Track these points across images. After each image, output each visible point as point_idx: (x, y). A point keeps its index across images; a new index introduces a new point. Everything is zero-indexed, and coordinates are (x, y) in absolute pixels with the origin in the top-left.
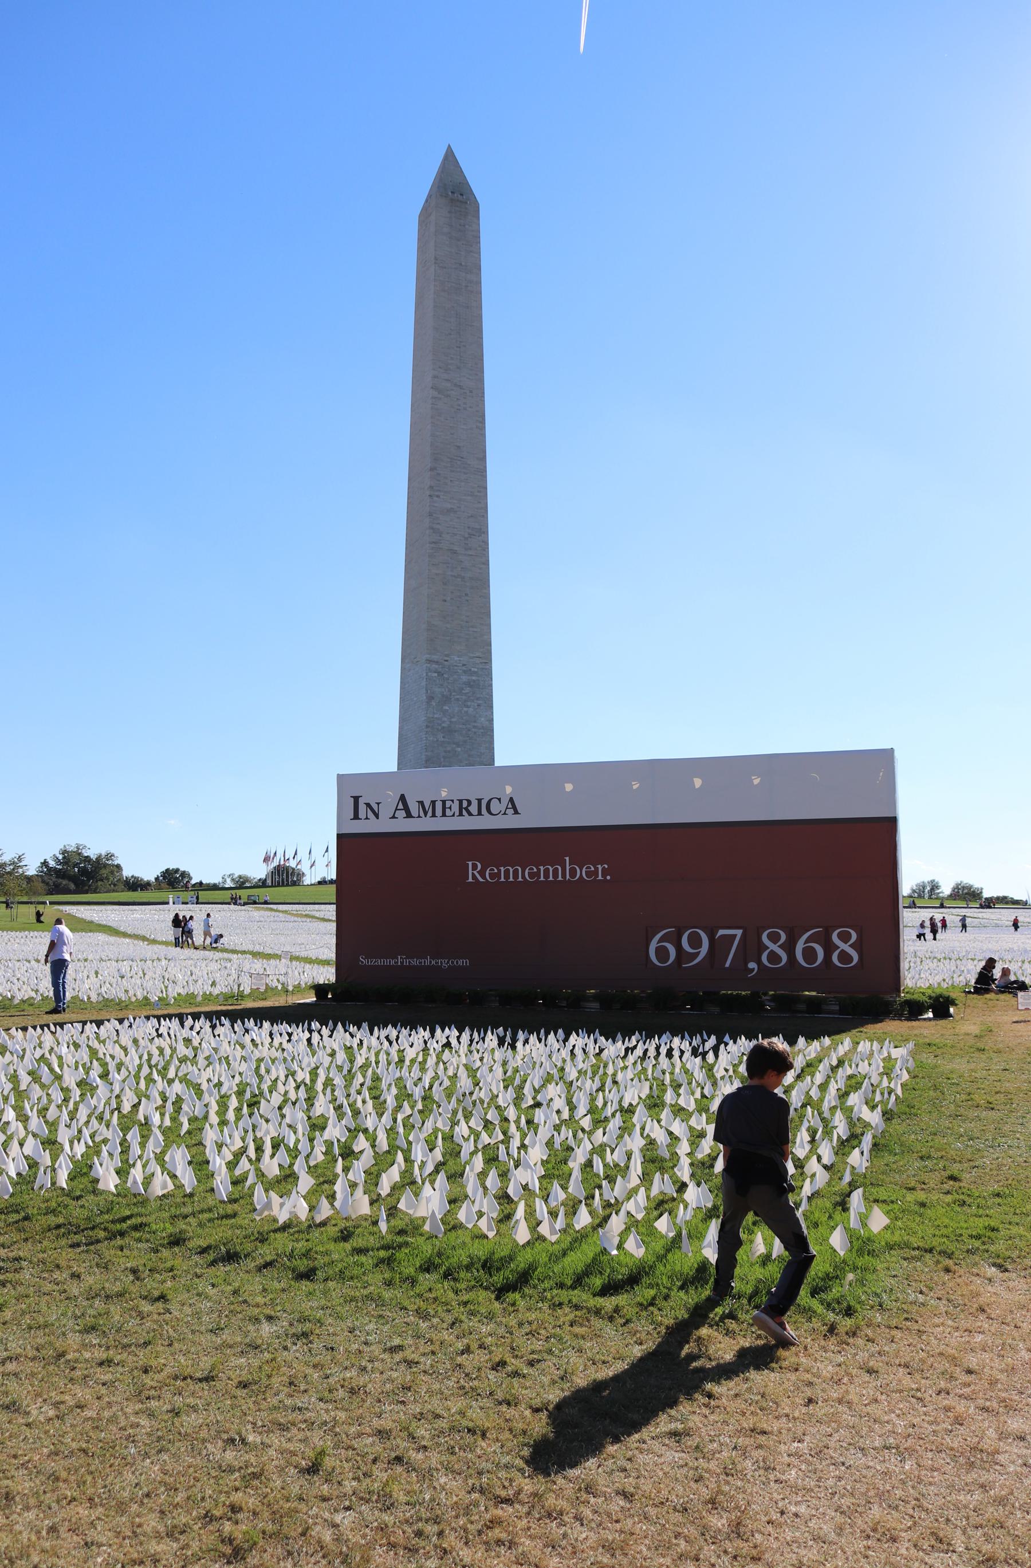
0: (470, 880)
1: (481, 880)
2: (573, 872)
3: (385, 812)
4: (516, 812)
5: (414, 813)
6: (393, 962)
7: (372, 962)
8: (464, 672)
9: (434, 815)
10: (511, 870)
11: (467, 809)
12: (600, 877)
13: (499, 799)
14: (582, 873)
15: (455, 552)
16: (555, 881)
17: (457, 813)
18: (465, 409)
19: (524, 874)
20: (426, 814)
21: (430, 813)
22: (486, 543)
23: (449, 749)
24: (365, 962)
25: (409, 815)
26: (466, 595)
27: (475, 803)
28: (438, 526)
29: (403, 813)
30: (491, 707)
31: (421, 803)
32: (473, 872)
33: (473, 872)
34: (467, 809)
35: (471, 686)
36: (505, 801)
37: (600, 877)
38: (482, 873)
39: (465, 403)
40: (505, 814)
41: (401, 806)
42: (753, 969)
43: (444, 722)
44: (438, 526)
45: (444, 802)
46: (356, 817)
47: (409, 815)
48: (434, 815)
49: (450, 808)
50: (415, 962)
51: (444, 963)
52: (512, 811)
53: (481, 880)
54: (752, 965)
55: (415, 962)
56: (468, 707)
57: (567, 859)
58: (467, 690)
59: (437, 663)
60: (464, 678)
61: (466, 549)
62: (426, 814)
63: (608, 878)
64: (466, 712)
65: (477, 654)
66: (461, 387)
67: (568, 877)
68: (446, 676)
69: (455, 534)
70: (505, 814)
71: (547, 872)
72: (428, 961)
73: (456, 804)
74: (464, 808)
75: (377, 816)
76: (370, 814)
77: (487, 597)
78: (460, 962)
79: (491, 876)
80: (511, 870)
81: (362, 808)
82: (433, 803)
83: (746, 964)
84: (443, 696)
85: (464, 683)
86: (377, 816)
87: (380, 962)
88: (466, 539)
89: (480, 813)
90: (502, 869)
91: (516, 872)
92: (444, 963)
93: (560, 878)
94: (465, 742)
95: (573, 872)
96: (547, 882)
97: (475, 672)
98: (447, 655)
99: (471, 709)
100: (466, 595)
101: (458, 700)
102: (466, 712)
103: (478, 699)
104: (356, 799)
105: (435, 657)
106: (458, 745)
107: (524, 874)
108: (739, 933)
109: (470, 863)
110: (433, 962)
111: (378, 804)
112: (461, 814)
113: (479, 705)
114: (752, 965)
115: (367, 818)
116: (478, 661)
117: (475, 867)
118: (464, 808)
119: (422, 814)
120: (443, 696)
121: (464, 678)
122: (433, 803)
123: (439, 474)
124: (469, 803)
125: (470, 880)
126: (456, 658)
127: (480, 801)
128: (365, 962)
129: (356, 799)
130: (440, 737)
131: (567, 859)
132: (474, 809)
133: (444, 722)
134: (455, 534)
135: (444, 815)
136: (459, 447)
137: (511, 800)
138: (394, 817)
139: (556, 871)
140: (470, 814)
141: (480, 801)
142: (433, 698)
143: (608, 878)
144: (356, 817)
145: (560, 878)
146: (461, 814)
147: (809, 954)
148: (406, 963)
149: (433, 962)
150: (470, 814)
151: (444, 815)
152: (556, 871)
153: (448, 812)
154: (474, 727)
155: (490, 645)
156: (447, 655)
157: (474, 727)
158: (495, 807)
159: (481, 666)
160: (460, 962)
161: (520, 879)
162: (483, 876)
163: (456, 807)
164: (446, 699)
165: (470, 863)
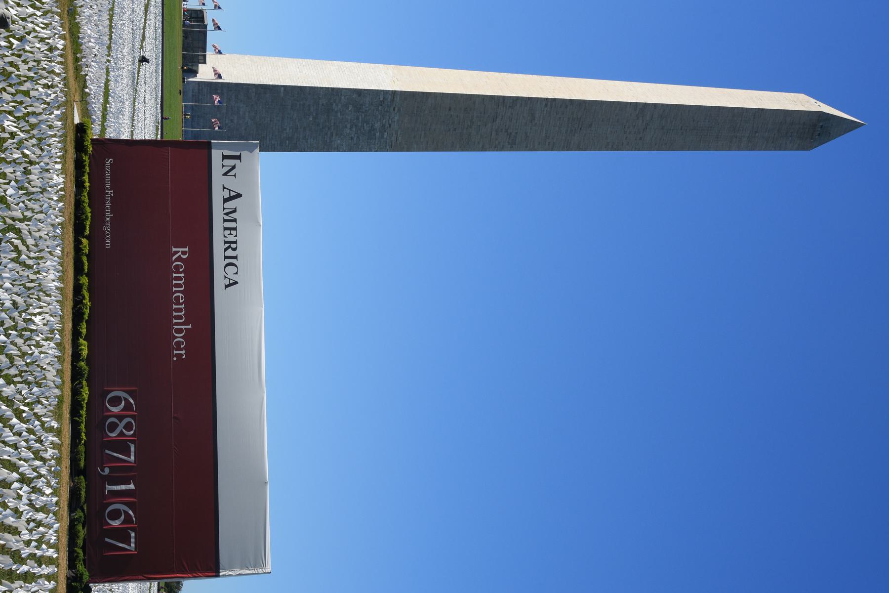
0: (174, 249)
1: (174, 258)
2: (179, 331)
3: (229, 182)
4: (226, 286)
5: (227, 205)
6: (108, 186)
7: (108, 169)
8: (384, 126)
9: (225, 221)
10: (181, 282)
11: (229, 247)
12: (175, 352)
14: (179, 338)
15: (494, 120)
17: (226, 239)
18: (625, 133)
19: (178, 293)
20: (227, 214)
21: (227, 218)
22: (502, 149)
23: (312, 109)
25: (226, 200)
26: (455, 130)
27: (233, 254)
29: (227, 196)
30: (351, 149)
31: (235, 211)
32: (180, 252)
34: (229, 247)
35: (370, 131)
36: (235, 278)
37: (175, 352)
39: (630, 133)
41: (233, 194)
43: (337, 105)
45: (235, 229)
46: (225, 157)
47: (226, 200)
48: (225, 221)
50: (108, 204)
52: (227, 283)
53: (174, 258)
55: (108, 204)
57: (190, 326)
58: (367, 128)
59: (393, 100)
60: (377, 125)
62: (227, 214)
64: (346, 127)
65: (400, 138)
66: (645, 129)
67: (176, 327)
68: (380, 108)
71: (179, 310)
73: (234, 239)
74: (230, 245)
75: (225, 174)
76: (226, 169)
77: (452, 148)
78: (108, 241)
79: (177, 267)
80: (181, 282)
81: (231, 162)
82: (235, 221)
86: (225, 174)
87: (108, 175)
88: (506, 131)
89: (226, 257)
90: (182, 275)
93: (175, 321)
95: (179, 331)
97: (383, 137)
98: (399, 110)
100: (455, 130)
101: (358, 119)
102: (346, 127)
103: (358, 137)
105: (398, 99)
107: (178, 293)
108: (133, 458)
109: (187, 249)
110: (108, 219)
112: (225, 242)
116: (393, 139)
117: (184, 253)
119: (226, 211)
121: (377, 125)
122: (235, 221)
123: (566, 107)
125: (174, 249)
127: (236, 258)
129: (239, 158)
131: (190, 326)
132: (230, 253)
133: (337, 105)
134: (511, 121)
136: (591, 126)
137: (236, 283)
138: (224, 188)
139: (180, 317)
140: (226, 250)
141: (236, 258)
142: (359, 96)
143: (175, 359)
144: (225, 157)
145: (175, 321)
147: (115, 515)
148: (108, 197)
149: (108, 219)
150: (226, 250)
151: (225, 229)
152: (180, 317)
153: (227, 232)
155: (408, 150)
156: (399, 110)
157: (332, 134)
160: (108, 241)
161: (174, 289)
162: (176, 260)
163: (231, 238)
165: (187, 249)
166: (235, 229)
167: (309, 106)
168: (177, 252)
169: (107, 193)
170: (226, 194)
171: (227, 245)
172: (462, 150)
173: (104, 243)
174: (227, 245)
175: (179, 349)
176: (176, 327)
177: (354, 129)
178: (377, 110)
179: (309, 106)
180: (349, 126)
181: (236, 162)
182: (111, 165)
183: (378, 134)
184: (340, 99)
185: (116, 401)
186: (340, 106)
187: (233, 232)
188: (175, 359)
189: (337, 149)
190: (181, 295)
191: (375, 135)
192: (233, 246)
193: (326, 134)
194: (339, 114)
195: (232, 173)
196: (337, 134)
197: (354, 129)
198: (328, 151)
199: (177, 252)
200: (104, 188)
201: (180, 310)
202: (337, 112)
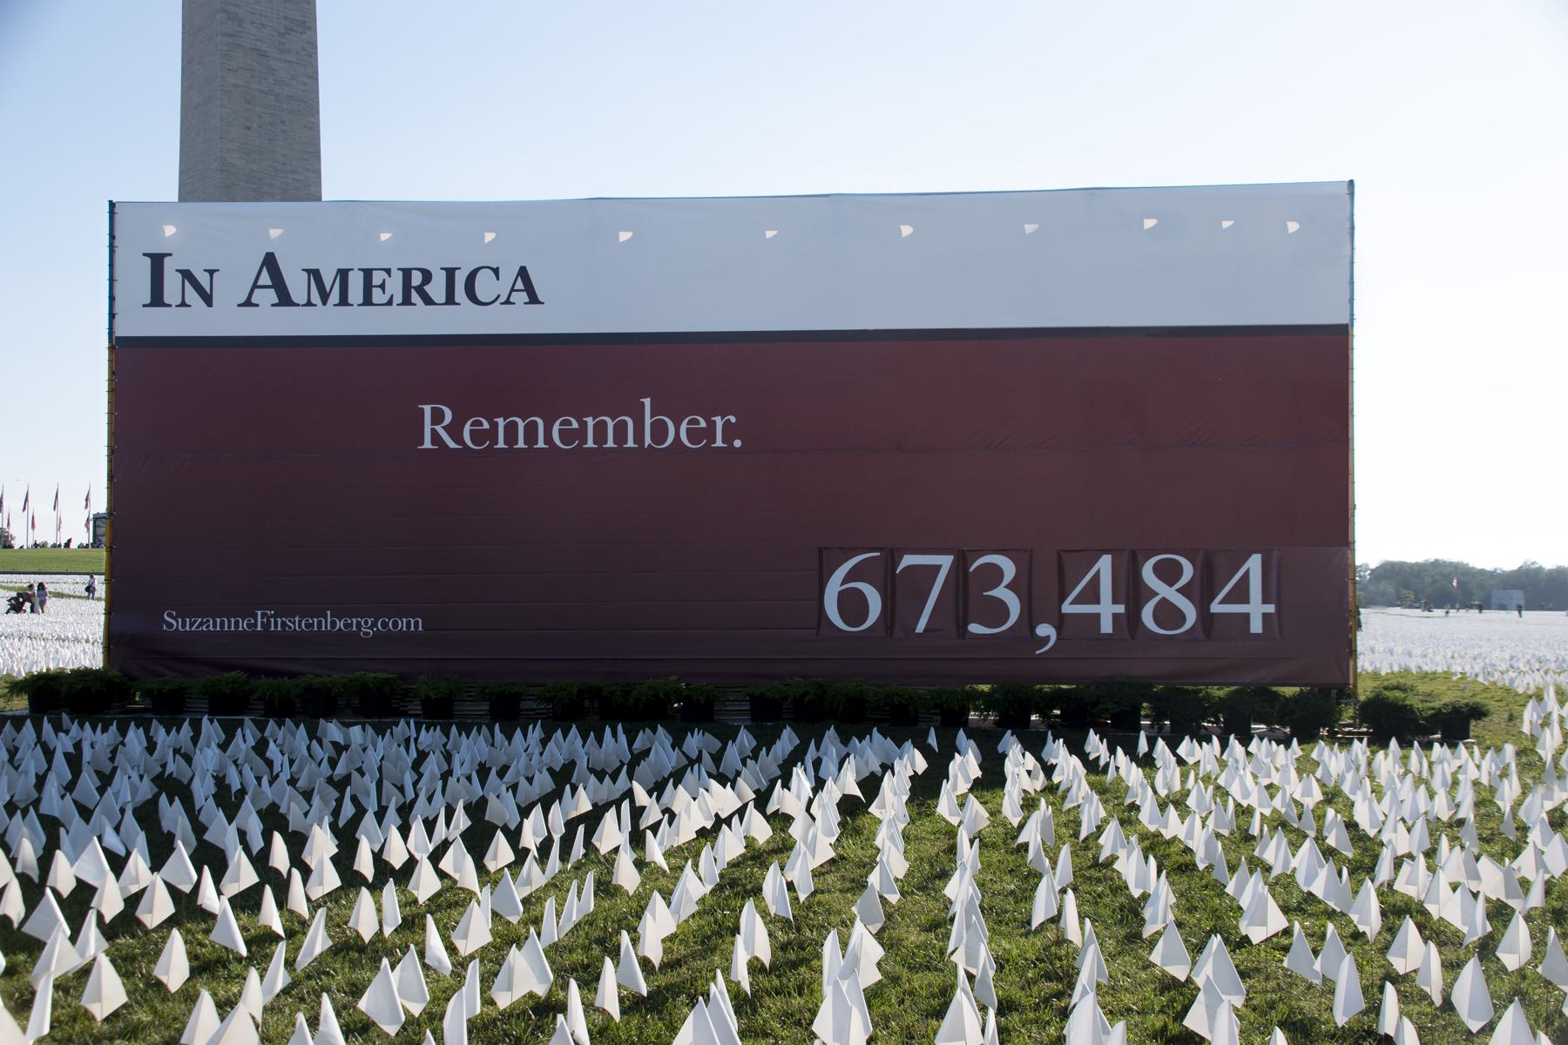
0: (428, 444)
1: (452, 444)
2: (659, 431)
3: (229, 290)
4: (534, 299)
6: (243, 625)
9: (344, 301)
10: (521, 425)
11: (420, 290)
12: (719, 443)
13: (496, 271)
14: (679, 432)
15: (264, 55)
16: (620, 450)
17: (398, 298)
19: (551, 434)
20: (325, 297)
21: (335, 297)
22: (315, 46)
24: (176, 624)
25: (285, 299)
27: (439, 280)
28: (236, 10)
31: (315, 274)
32: (435, 427)
33: (435, 427)
34: (420, 290)
36: (509, 274)
37: (719, 443)
38: (455, 430)
40: (508, 302)
41: (265, 279)
42: (1047, 638)
44: (236, 10)
45: (368, 274)
46: (157, 299)
47: (285, 299)
48: (344, 301)
49: (382, 286)
50: (297, 624)
51: (366, 627)
52: (524, 297)
53: (452, 444)
54: (1045, 630)
55: (297, 624)
57: (647, 401)
61: (282, 52)
62: (325, 297)
63: (737, 443)
67: (648, 441)
69: (264, 26)
70: (508, 302)
71: (601, 431)
72: (325, 623)
73: (398, 277)
74: (414, 288)
75: (208, 299)
76: (192, 296)
78: (402, 624)
80: (521, 425)
82: (343, 274)
83: (1032, 629)
86: (208, 299)
87: (212, 625)
88: (282, 35)
89: (450, 300)
91: (531, 431)
92: (366, 627)
93: (630, 443)
95: (659, 431)
96: (601, 450)
100: (283, 122)
104: (157, 261)
107: (551, 434)
109: (427, 409)
110: (340, 624)
111: (211, 272)
112: (407, 301)
114: (1045, 630)
115: (183, 304)
117: (437, 417)
118: (414, 288)
119: (316, 298)
122: (343, 274)
124: (427, 276)
125: (428, 444)
127: (450, 273)
128: (176, 624)
129: (157, 261)
131: (647, 401)
132: (437, 289)
134: (264, 26)
135: (367, 301)
137: (523, 273)
138: (248, 303)
140: (428, 301)
141: (450, 273)
144: (157, 299)
145: (630, 443)
146: (407, 301)
148: (276, 625)
149: (340, 624)
150: (428, 301)
151: (367, 301)
153: (377, 296)
158: (486, 286)
160: (402, 624)
161: (541, 444)
162: (458, 438)
163: (395, 286)
165: (427, 409)
166: (368, 274)
168: (436, 437)
169: (266, 626)
170: (267, 297)
171: (415, 297)
172: (318, 112)
173: (406, 636)
174: (415, 297)
175: (710, 432)
176: (648, 441)
181: (170, 267)
182: (182, 615)
185: (853, 605)
187: (377, 278)
188: (737, 443)
190: (556, 427)
192: (417, 279)
195: (204, 280)
199: (436, 437)
200: (251, 636)
201: (600, 429)
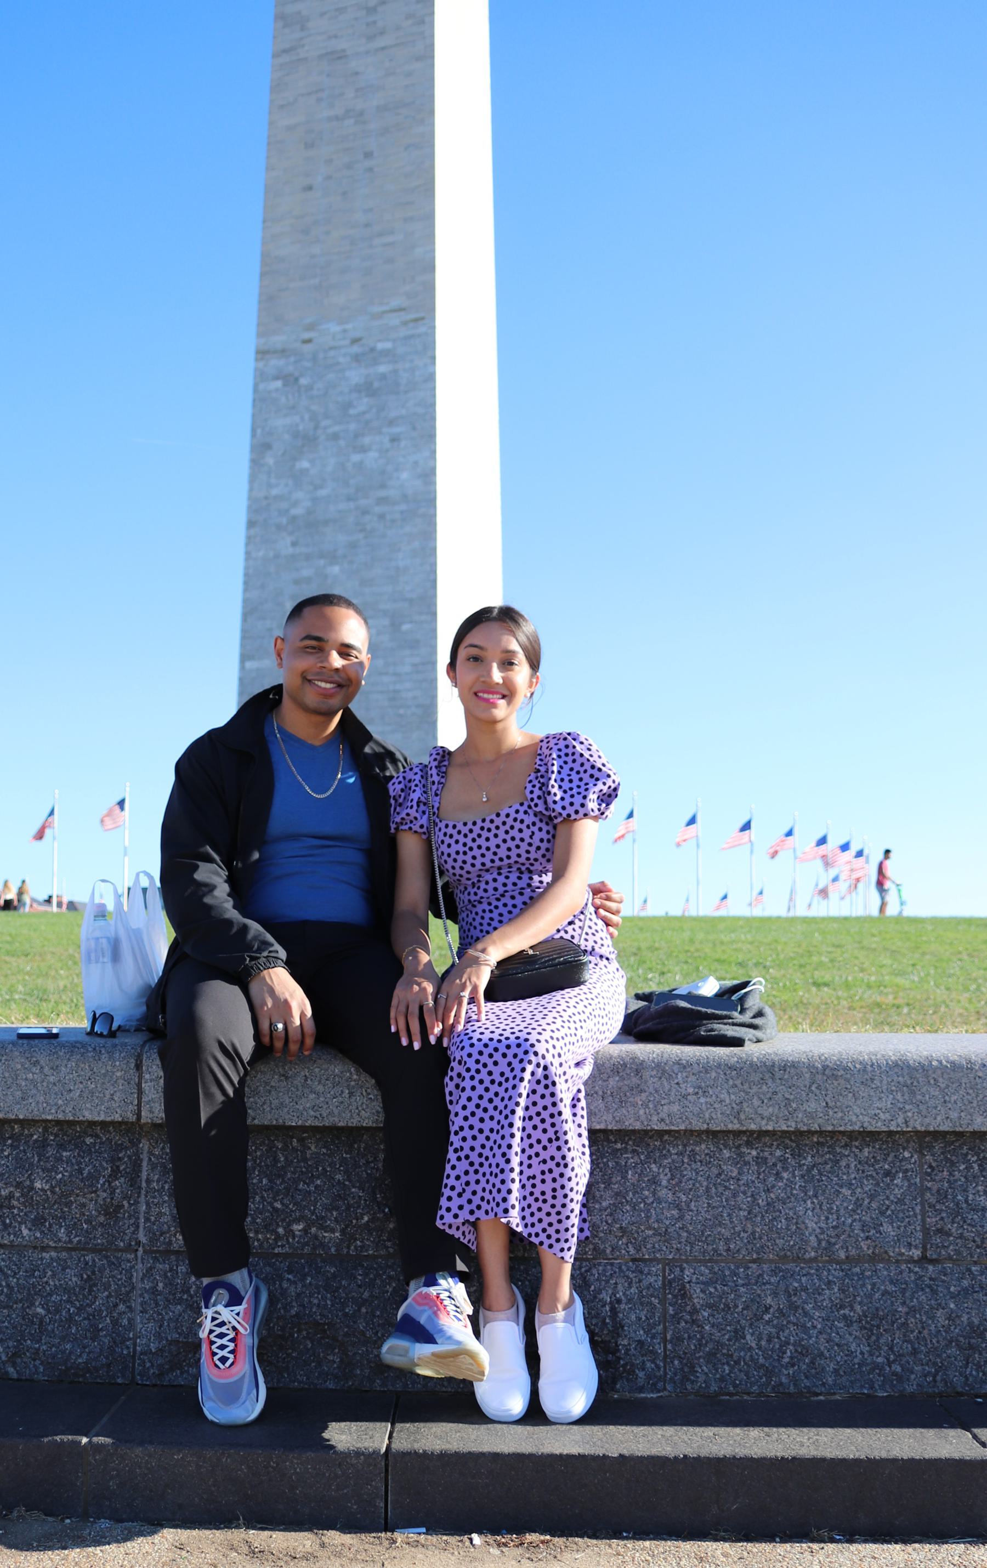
8: (357, 358)
15: (340, 56)
23: (306, 573)
26: (368, 155)
30: (430, 436)
43: (295, 504)
56: (364, 450)
58: (363, 404)
59: (283, 352)
60: (355, 376)
61: (371, 38)
64: (360, 466)
65: (395, 303)
68: (303, 381)
84: (296, 435)
85: (357, 389)
94: (353, 546)
97: (386, 353)
98: (311, 327)
99: (373, 454)
100: (368, 155)
101: (335, 437)
102: (360, 466)
103: (391, 423)
105: (278, 340)
106: (332, 558)
113: (395, 439)
116: (394, 320)
120: (296, 435)
126: (334, 328)
130: (284, 545)
133: (295, 504)
142: (267, 446)
154: (381, 501)
156: (311, 327)
157: (381, 501)
159: (403, 332)
164: (306, 441)
167: (297, 582)
172: (432, 112)
177: (367, 440)
178: (309, 388)
179: (297, 582)
180: (356, 458)
183: (382, 369)
184: (278, 498)
186: (299, 495)
189: (428, 475)
191: (383, 377)
193: (382, 517)
194: (323, 493)
196: (383, 486)
197: (367, 440)
198: (430, 501)
202: (315, 500)
